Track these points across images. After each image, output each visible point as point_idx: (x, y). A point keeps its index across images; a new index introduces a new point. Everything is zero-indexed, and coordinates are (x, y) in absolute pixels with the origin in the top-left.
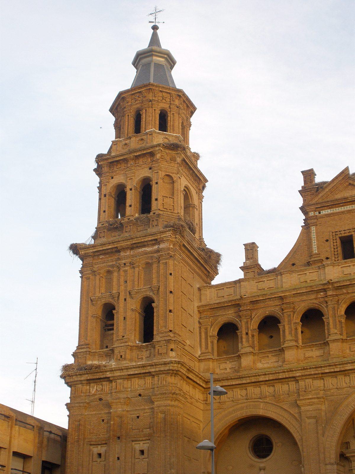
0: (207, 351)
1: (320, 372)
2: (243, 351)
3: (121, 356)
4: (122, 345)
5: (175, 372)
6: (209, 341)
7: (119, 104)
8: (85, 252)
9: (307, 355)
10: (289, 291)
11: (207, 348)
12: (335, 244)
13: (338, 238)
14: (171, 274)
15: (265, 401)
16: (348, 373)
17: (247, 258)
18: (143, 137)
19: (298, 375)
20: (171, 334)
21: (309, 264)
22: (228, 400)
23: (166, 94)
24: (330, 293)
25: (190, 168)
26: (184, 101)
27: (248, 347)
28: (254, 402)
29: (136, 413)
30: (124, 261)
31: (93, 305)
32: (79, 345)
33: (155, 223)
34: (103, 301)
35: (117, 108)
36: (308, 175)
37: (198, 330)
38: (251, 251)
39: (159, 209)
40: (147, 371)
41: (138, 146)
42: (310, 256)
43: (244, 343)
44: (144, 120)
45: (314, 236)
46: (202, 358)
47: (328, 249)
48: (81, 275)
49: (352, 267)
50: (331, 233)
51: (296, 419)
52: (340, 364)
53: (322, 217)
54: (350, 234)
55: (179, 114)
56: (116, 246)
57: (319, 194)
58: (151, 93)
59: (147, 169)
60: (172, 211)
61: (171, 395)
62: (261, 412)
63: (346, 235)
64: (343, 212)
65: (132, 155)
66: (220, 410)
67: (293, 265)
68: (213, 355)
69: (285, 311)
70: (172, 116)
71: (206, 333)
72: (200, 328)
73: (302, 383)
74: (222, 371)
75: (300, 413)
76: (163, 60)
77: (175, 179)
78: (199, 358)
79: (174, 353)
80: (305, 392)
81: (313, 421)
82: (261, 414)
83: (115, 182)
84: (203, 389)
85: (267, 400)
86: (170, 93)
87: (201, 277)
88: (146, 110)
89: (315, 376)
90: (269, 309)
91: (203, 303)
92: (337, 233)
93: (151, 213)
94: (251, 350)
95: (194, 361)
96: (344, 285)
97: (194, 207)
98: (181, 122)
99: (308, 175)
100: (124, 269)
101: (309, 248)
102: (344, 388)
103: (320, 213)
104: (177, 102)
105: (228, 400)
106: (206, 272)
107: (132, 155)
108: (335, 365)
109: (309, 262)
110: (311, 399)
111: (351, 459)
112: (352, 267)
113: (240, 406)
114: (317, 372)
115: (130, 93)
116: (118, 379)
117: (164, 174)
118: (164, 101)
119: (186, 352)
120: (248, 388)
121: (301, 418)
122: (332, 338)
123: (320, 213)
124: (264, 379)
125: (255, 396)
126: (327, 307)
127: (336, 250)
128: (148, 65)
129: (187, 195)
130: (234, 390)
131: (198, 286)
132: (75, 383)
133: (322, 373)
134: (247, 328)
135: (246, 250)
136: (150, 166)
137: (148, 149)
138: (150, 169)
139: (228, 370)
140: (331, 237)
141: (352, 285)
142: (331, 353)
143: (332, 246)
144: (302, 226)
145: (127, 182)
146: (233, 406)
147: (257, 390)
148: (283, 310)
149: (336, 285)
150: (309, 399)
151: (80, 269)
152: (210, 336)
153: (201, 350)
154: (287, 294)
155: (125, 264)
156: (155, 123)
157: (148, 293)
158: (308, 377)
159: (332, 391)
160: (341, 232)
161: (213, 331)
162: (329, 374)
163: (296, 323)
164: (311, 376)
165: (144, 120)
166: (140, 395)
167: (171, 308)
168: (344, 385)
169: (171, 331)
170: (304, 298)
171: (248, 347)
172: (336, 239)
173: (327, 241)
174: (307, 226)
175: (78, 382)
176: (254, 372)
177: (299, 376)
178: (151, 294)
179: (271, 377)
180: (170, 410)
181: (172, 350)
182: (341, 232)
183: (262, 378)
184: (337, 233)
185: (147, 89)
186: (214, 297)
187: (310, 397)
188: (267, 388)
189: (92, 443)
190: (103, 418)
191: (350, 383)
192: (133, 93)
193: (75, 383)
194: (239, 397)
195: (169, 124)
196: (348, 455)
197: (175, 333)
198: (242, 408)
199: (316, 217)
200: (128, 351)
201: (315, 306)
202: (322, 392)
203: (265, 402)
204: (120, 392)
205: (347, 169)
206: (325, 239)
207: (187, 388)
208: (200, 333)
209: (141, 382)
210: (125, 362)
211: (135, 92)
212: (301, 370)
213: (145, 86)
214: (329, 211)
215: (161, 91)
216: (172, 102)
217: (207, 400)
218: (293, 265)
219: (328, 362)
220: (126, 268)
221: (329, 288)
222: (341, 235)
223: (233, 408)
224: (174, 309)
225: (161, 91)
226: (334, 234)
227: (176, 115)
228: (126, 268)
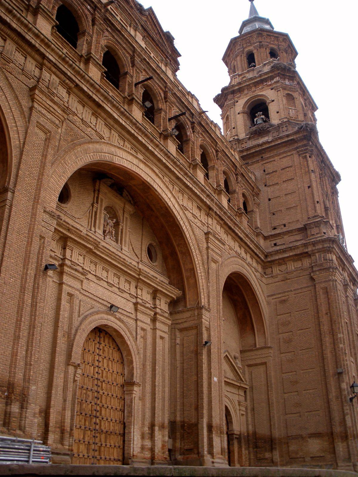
16: (99, 114)
51: (22, 112)
52: (103, 95)
73: (46, 75)
75: (31, 109)
81: (42, 135)
89: (67, 81)
96: (112, 24)
108: (98, 91)
121: (30, 114)
133: (77, 86)
141: (119, 34)
149: (108, 15)
158: (58, 73)
162: (82, 96)
164: (63, 77)
177: (50, 61)
201: (79, 10)
212: (60, 57)
221: (100, 10)
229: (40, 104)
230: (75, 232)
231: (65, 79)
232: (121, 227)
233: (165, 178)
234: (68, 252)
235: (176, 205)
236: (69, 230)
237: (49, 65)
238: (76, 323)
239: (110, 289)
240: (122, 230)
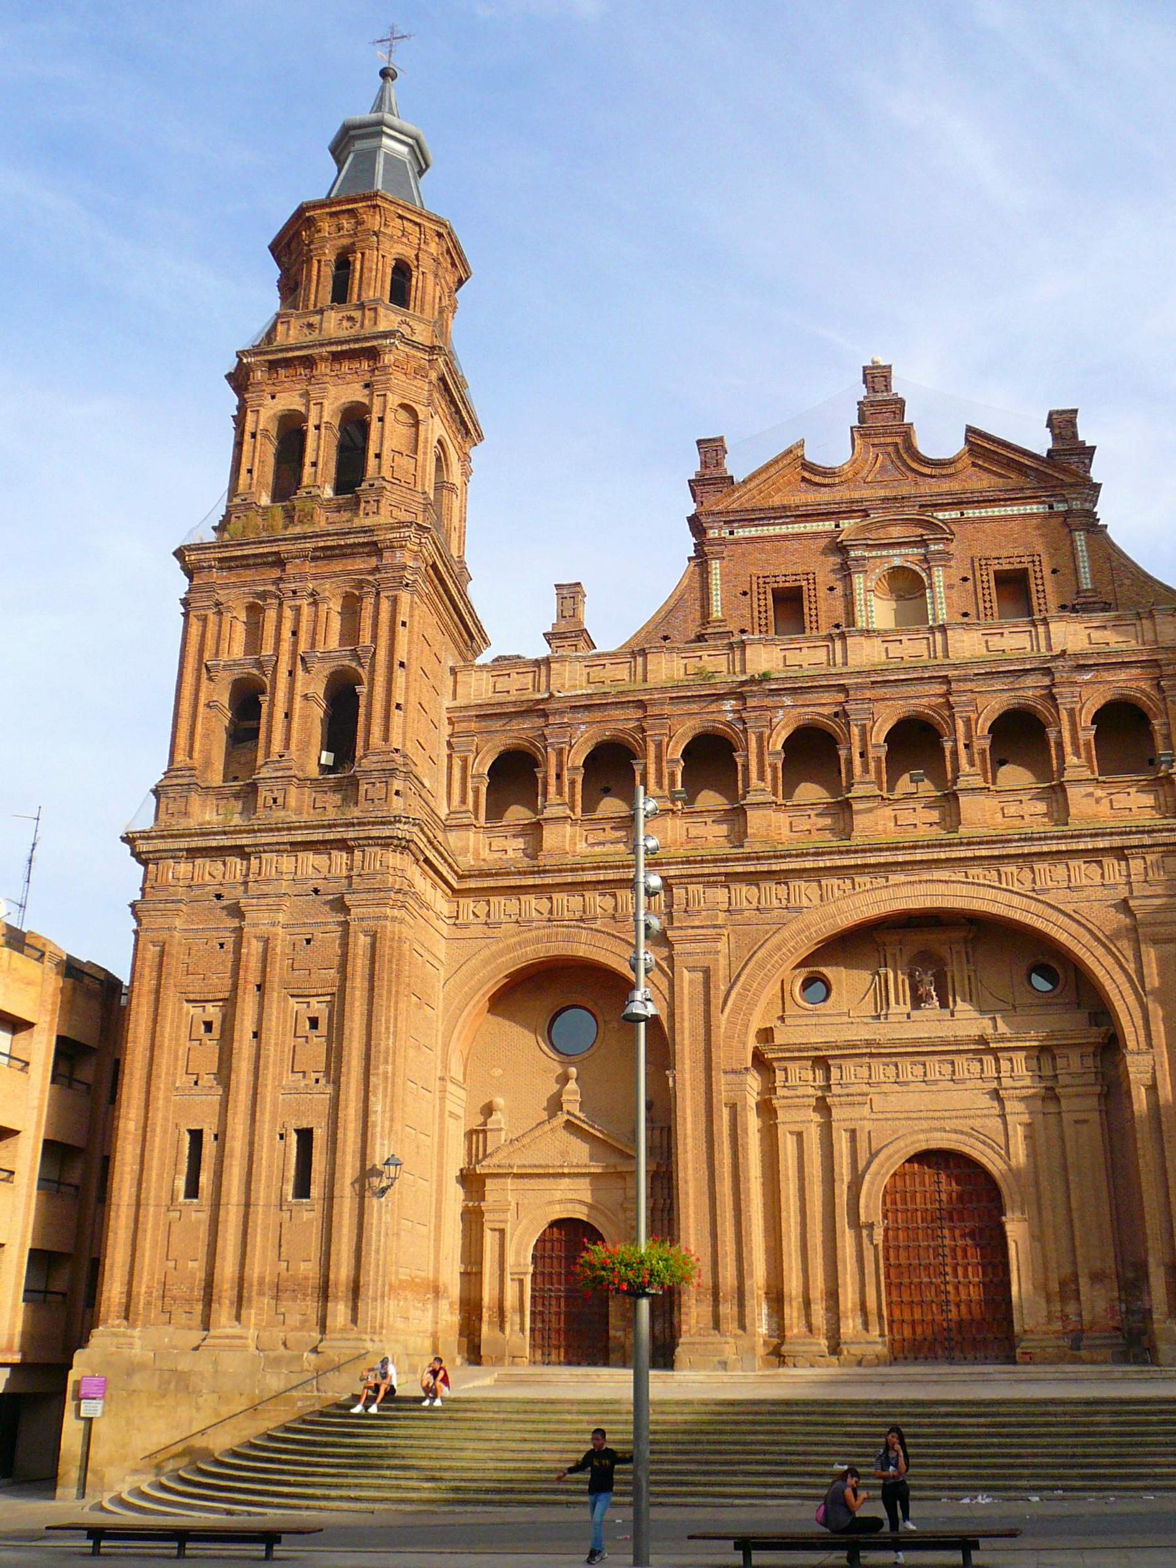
0: (464, 808)
1: (722, 870)
2: (548, 813)
3: (275, 800)
4: (280, 774)
5: (404, 843)
6: (470, 786)
7: (298, 234)
8: (198, 557)
9: (693, 833)
10: (663, 689)
11: (463, 801)
12: (762, 603)
13: (769, 591)
14: (404, 624)
15: (593, 926)
17: (561, 616)
18: (353, 314)
19: (672, 873)
20: (396, 756)
21: (700, 638)
22: (507, 919)
23: (410, 225)
24: (751, 702)
25: (453, 401)
26: (448, 252)
27: (559, 805)
28: (568, 927)
29: (303, 930)
30: (293, 586)
31: (210, 679)
32: (169, 770)
33: (372, 507)
34: (237, 673)
35: (289, 244)
36: (711, 449)
37: (446, 759)
38: (570, 602)
39: (383, 478)
40: (339, 836)
41: (343, 334)
42: (703, 624)
43: (549, 797)
44: (357, 275)
45: (715, 580)
46: (454, 822)
47: (747, 612)
48: (183, 611)
49: (805, 651)
50: (754, 579)
53: (737, 542)
54: (798, 584)
55: (436, 276)
56: (275, 549)
57: (734, 491)
58: (378, 217)
59: (358, 386)
60: (411, 486)
61: (393, 895)
62: (582, 951)
63: (787, 585)
64: (785, 537)
65: (324, 351)
66: (487, 941)
67: (666, 638)
68: (477, 818)
69: (649, 733)
70: (421, 277)
71: (464, 769)
72: (450, 757)
74: (497, 855)
76: (404, 150)
77: (421, 417)
78: (447, 823)
79: (401, 800)
80: (686, 911)
82: (581, 954)
83: (280, 407)
85: (598, 925)
86: (419, 225)
87: (457, 646)
88: (363, 254)
89: (712, 879)
90: (612, 725)
91: (460, 702)
92: (767, 580)
93: (364, 485)
94: (568, 812)
97: (452, 489)
98: (438, 294)
99: (711, 449)
100: (293, 603)
101: (702, 607)
102: (773, 909)
103: (731, 533)
104: (433, 248)
105: (507, 919)
106: (466, 637)
107: (324, 351)
109: (703, 635)
110: (698, 927)
111: (775, 1064)
112: (805, 651)
113: (534, 933)
114: (716, 870)
115: (328, 210)
116: (265, 852)
118: (405, 240)
120: (555, 896)
122: (750, 799)
123: (731, 533)
124: (594, 878)
125: (571, 916)
126: (745, 731)
127: (763, 615)
128: (371, 155)
129: (441, 462)
130: (522, 897)
131: (451, 664)
132: (158, 855)
133: (727, 874)
134: (560, 765)
135: (562, 599)
136: (367, 377)
137: (366, 339)
138: (367, 386)
139: (511, 854)
140: (755, 587)
142: (749, 831)
143: (755, 606)
144: (690, 559)
145: (308, 410)
146: (518, 934)
147: (576, 902)
148: (644, 731)
150: (693, 927)
151: (183, 596)
152: (473, 777)
153: (449, 806)
154: (656, 696)
155: (294, 592)
156: (382, 287)
157: (347, 663)
158: (694, 880)
159: (746, 913)
160: (778, 579)
161: (479, 764)
162: (746, 878)
163: (672, 761)
164: (701, 879)
165: (357, 275)
166: (316, 891)
167: (401, 701)
168: (775, 902)
169: (397, 750)
170: (694, 707)
171: (559, 805)
172: (765, 593)
173: (745, 594)
174: (701, 559)
175: (164, 855)
176: (569, 859)
177: (675, 877)
178: (354, 664)
179: (611, 875)
180: (386, 927)
181: (397, 793)
182: (778, 579)
183: (589, 876)
184: (767, 580)
185: (369, 206)
186: (487, 691)
187: (697, 923)
188: (598, 898)
189: (192, 997)
190: (222, 941)
191: (788, 900)
192: (334, 209)
193: (158, 855)
194: (534, 913)
195: (413, 293)
196: (770, 1056)
197: (405, 756)
198: (538, 940)
199: (721, 541)
200: (293, 790)
202: (722, 915)
203: (592, 929)
204: (268, 881)
205: (801, 445)
206: (740, 590)
207: (423, 884)
208: (450, 768)
209: (320, 860)
210: (282, 813)
211: (338, 209)
212: (682, 863)
213: (365, 198)
214: (753, 532)
215: (401, 217)
216: (422, 246)
217: (457, 918)
218: (666, 638)
219: (741, 850)
220: (298, 603)
222: (776, 585)
223: (517, 939)
224: (407, 701)
225: (401, 217)
226: (761, 581)
227: (430, 278)
228: (298, 603)
229: (682, 941)
231: (706, 879)
232: (949, 975)
233: (971, 872)
234: (835, 1072)
235: (1016, 900)
236: (817, 1049)
237: (677, 881)
238: (861, 1165)
239: (934, 1088)
240: (953, 977)
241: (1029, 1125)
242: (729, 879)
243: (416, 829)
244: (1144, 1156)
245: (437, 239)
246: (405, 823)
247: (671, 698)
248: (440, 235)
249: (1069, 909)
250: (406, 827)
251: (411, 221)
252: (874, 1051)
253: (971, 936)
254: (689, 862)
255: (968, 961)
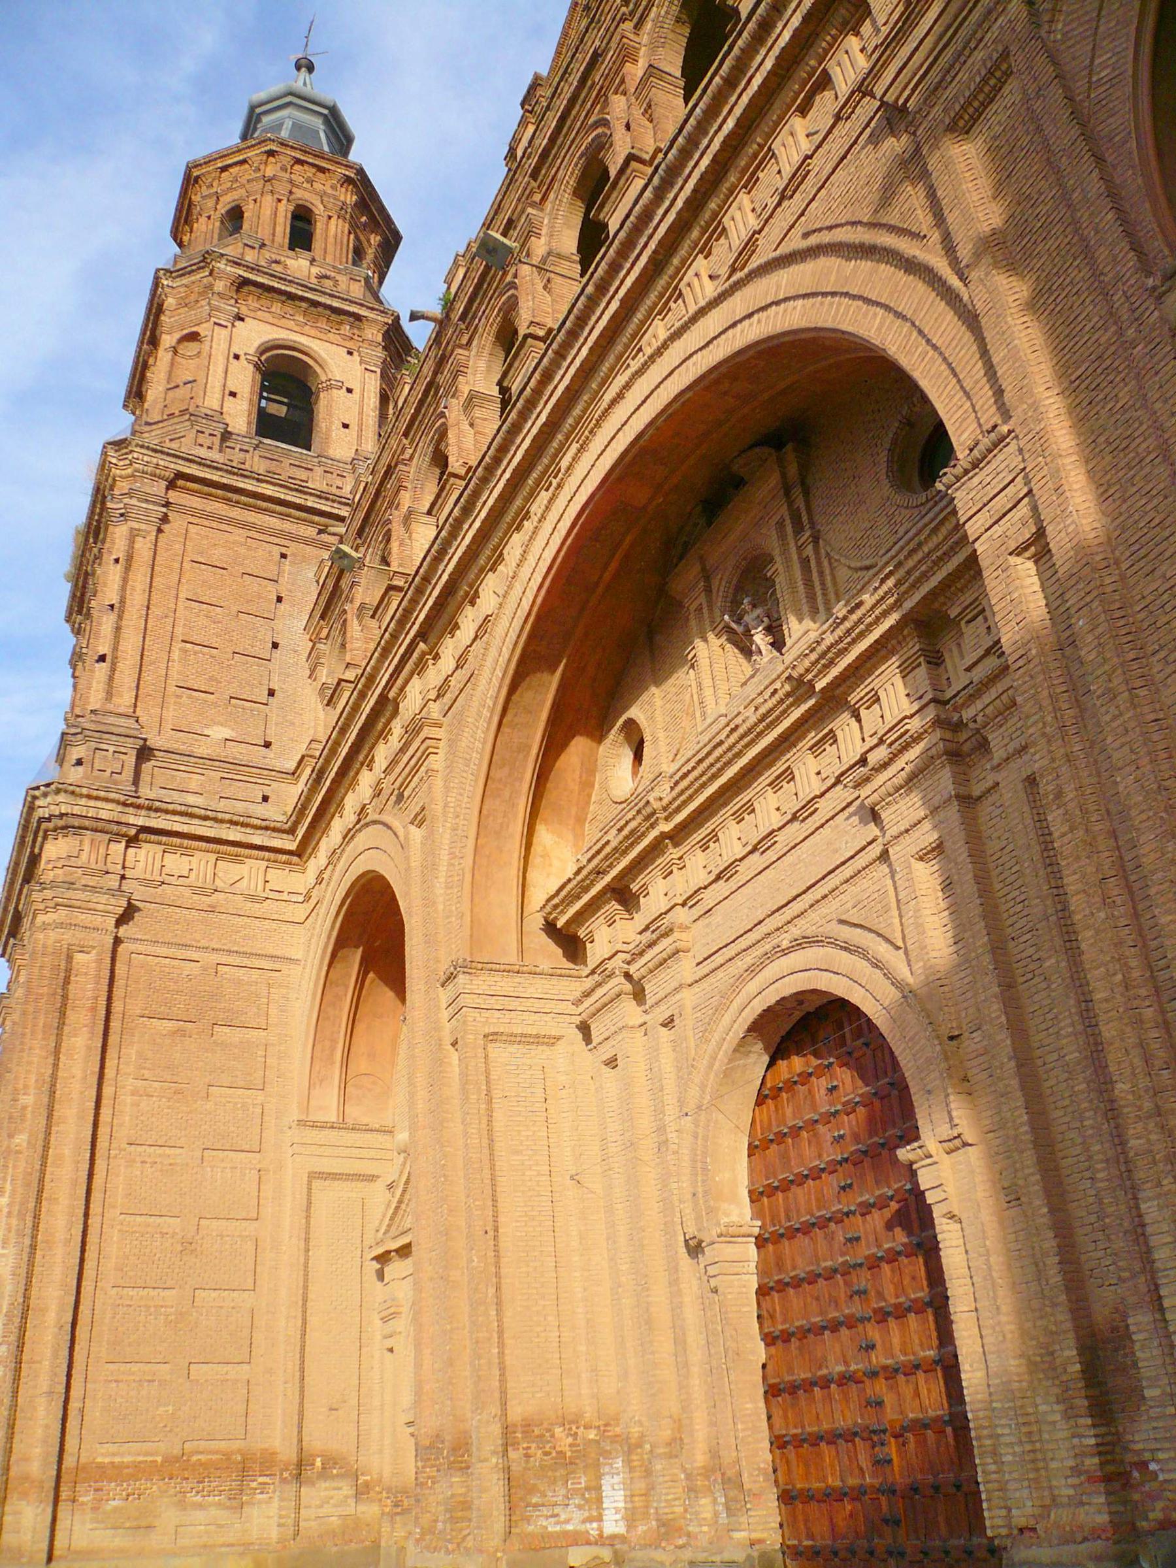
84: (295, 859)
95: (267, 782)
117: (177, 336)
119: (193, 760)
215: (224, 169)
225: (224, 169)
230: (606, 858)
236: (599, 872)
241: (938, 849)
242: (432, 639)
243: (61, 798)
244: (1059, 795)
245: (271, 159)
246: (45, 795)
247: (406, 435)
248: (271, 153)
249: (796, 242)
250: (49, 799)
251: (236, 164)
252: (666, 827)
253: (793, 470)
254: (386, 652)
255: (798, 528)
